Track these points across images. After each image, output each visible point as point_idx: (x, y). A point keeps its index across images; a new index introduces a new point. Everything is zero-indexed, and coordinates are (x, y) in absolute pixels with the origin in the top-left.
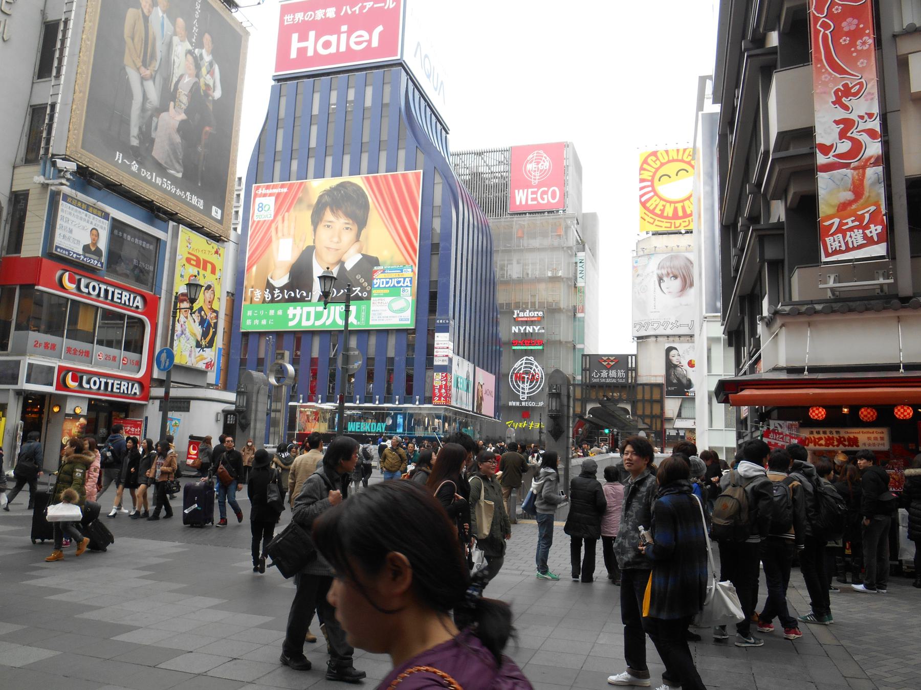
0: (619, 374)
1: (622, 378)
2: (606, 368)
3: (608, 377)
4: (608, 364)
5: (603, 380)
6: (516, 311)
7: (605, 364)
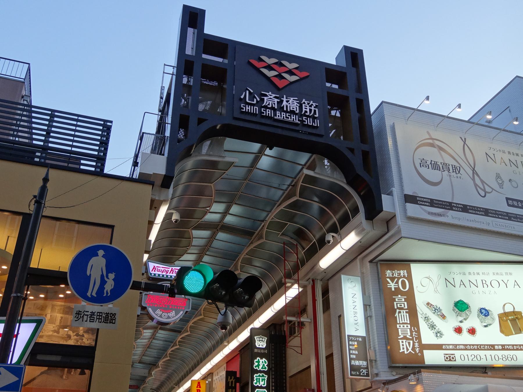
0: (306, 108)
5: (269, 112)
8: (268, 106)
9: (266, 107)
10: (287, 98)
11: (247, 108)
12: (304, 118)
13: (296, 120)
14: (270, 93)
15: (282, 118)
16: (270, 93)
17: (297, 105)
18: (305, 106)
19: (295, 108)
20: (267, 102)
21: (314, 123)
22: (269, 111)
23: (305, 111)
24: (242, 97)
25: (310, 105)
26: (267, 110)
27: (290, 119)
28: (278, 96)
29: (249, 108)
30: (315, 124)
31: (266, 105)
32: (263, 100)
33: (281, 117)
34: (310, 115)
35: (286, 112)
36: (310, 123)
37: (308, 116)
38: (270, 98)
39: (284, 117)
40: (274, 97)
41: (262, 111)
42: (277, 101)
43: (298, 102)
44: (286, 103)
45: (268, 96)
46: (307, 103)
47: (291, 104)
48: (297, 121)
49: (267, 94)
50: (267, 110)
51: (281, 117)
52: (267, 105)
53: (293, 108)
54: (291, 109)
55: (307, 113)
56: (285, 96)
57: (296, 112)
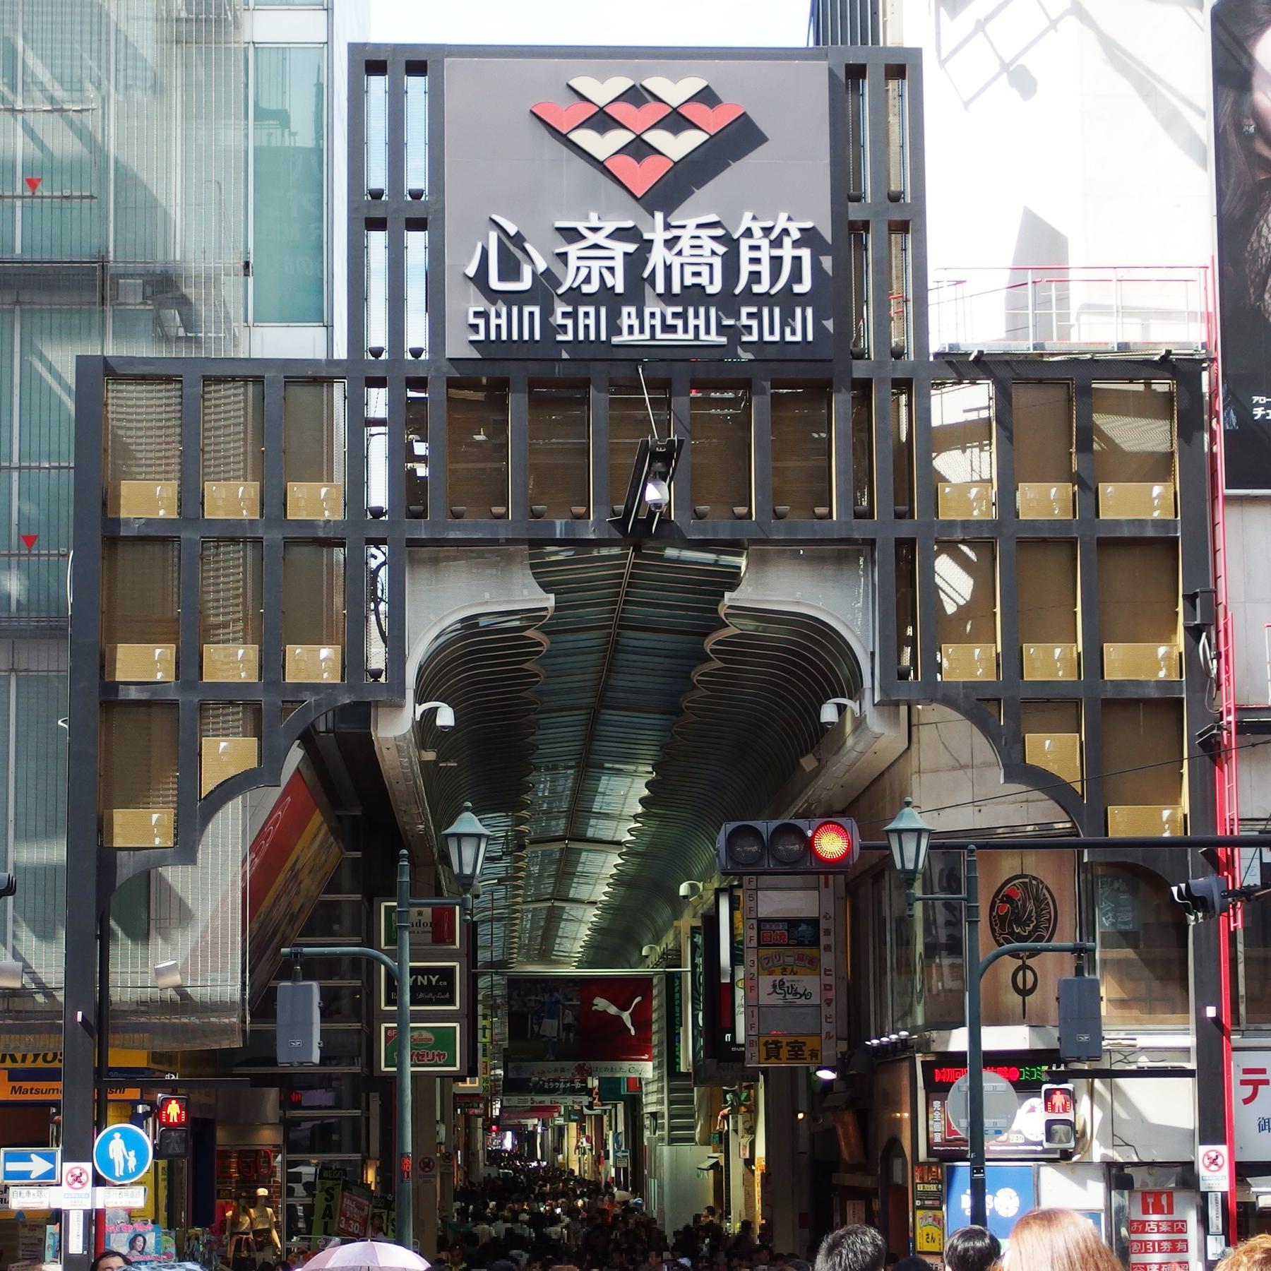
1: (787, 301)
4: (639, 149)
5: (590, 321)
7: (603, 145)
8: (586, 289)
9: (575, 296)
10: (668, 226)
11: (494, 322)
12: (745, 311)
13: (708, 332)
15: (647, 335)
17: (713, 253)
18: (753, 248)
19: (705, 270)
20: (578, 268)
21: (788, 330)
22: (587, 315)
23: (751, 273)
25: (774, 235)
26: (582, 310)
27: (680, 335)
29: (503, 322)
30: (793, 333)
31: (575, 286)
33: (642, 331)
34: (773, 292)
36: (772, 332)
37: (765, 299)
38: (596, 246)
39: (653, 327)
40: (609, 237)
42: (626, 254)
43: (720, 232)
44: (665, 251)
45: (584, 238)
46: (764, 229)
47: (687, 251)
49: (581, 226)
50: (582, 310)
51: (642, 331)
52: (579, 287)
54: (689, 281)
55: (759, 282)
57: (711, 290)
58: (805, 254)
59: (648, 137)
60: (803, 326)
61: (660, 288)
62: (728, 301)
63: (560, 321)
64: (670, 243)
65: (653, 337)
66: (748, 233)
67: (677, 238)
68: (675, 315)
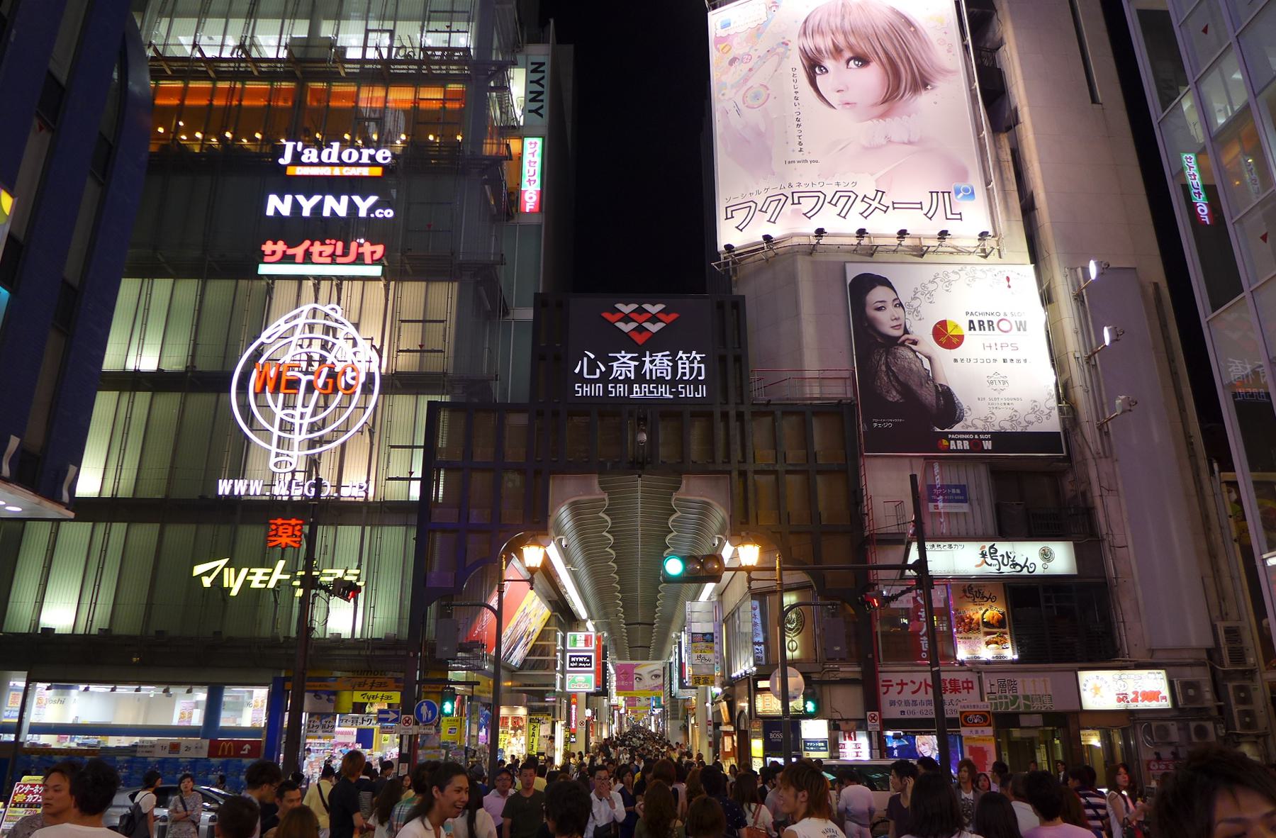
0: (683, 367)
1: (696, 382)
2: (626, 343)
3: (640, 378)
4: (641, 329)
5: (621, 390)
6: (289, 146)
7: (627, 328)
8: (620, 378)
9: (616, 381)
10: (651, 356)
11: (585, 389)
14: (623, 353)
16: (623, 353)
17: (668, 365)
18: (682, 364)
19: (665, 371)
24: (577, 371)
28: (636, 355)
29: (588, 389)
32: (610, 369)
35: (650, 381)
37: (688, 382)
38: (624, 363)
39: (645, 392)
41: (610, 389)
43: (670, 358)
48: (668, 395)
49: (618, 355)
53: (661, 373)
54: (659, 375)
56: (648, 353)
57: (667, 378)
58: (702, 366)
59: (644, 324)
60: (703, 392)
61: (648, 378)
62: (673, 383)
63: (610, 389)
64: (652, 362)
65: (645, 395)
66: (681, 358)
67: (655, 360)
68: (653, 388)
